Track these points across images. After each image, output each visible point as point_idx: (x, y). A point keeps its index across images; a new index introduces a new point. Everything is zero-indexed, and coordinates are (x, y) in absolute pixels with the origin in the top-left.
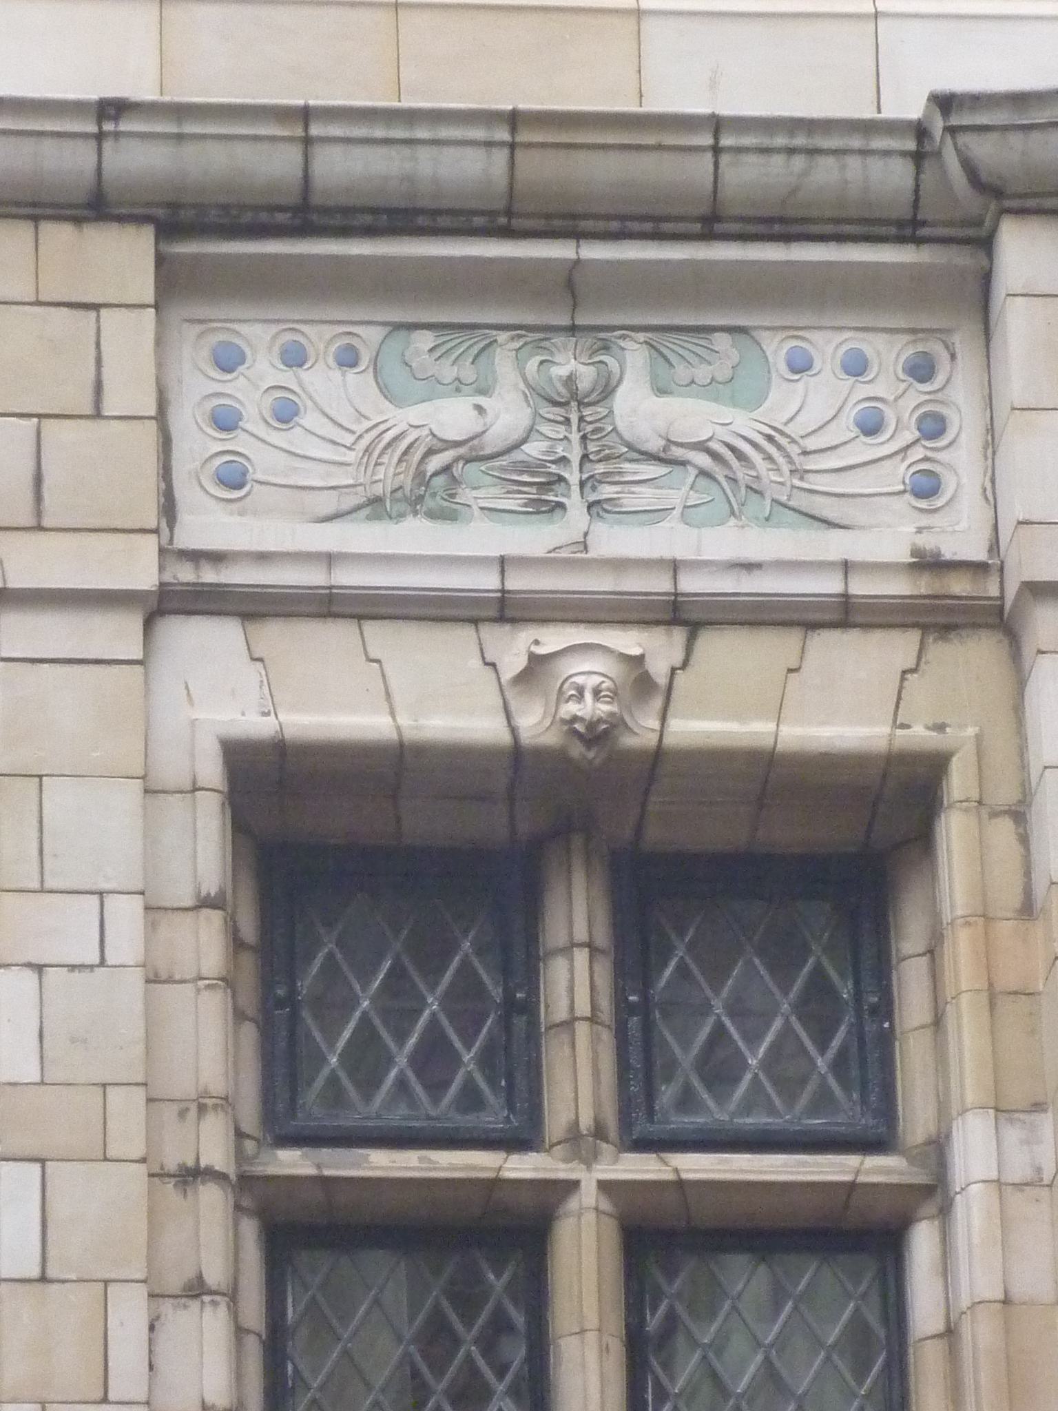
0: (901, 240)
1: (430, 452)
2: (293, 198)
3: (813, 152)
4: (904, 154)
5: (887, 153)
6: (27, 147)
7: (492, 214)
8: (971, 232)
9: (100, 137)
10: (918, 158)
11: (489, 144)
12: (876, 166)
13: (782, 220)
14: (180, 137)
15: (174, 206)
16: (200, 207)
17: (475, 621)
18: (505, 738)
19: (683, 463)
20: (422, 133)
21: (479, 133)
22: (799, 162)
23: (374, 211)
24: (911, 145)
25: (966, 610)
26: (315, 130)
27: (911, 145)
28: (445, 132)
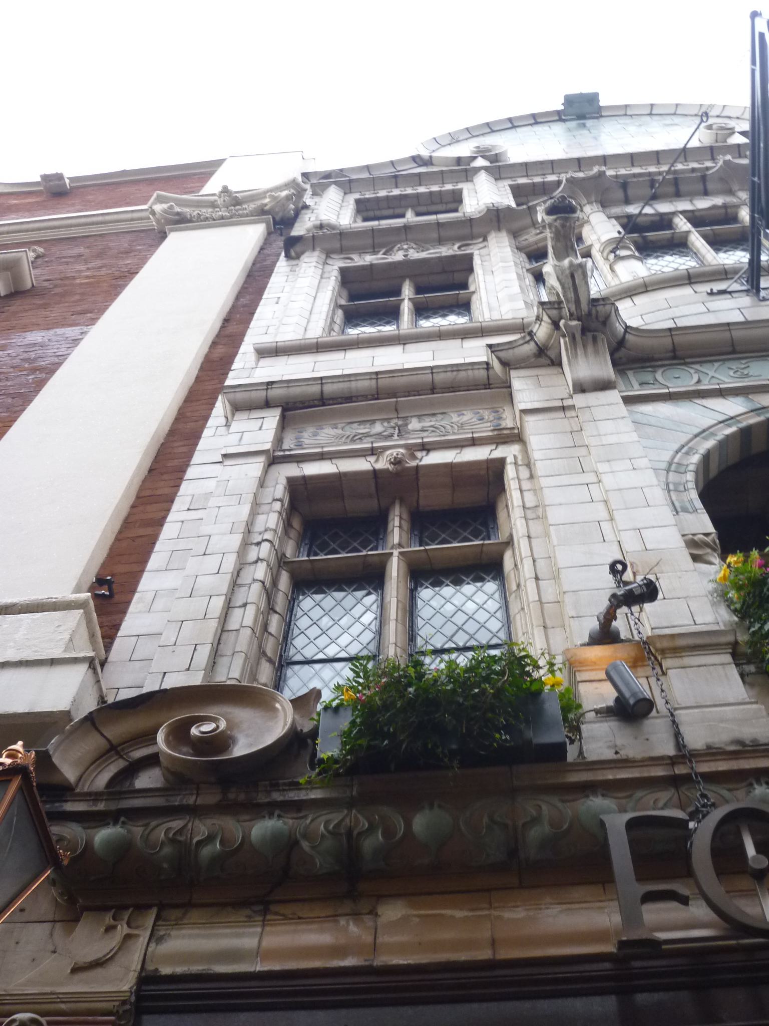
0: (486, 389)
1: (355, 436)
2: (318, 396)
3: (458, 371)
4: (483, 368)
5: (479, 369)
6: (248, 393)
7: (373, 395)
8: (506, 385)
9: (267, 389)
10: (488, 369)
11: (370, 379)
12: (476, 372)
13: (452, 387)
14: (288, 387)
15: (287, 403)
16: (295, 403)
17: (365, 456)
18: (371, 468)
19: (427, 431)
20: (352, 379)
21: (368, 377)
22: (455, 373)
23: (342, 398)
24: (485, 366)
25: (508, 437)
26: (324, 381)
27: (485, 366)
28: (358, 378)
